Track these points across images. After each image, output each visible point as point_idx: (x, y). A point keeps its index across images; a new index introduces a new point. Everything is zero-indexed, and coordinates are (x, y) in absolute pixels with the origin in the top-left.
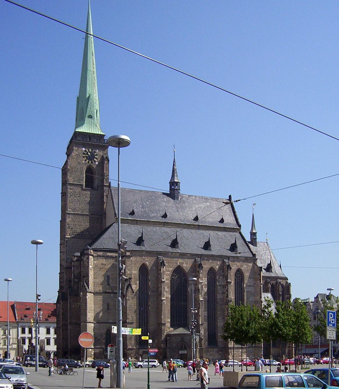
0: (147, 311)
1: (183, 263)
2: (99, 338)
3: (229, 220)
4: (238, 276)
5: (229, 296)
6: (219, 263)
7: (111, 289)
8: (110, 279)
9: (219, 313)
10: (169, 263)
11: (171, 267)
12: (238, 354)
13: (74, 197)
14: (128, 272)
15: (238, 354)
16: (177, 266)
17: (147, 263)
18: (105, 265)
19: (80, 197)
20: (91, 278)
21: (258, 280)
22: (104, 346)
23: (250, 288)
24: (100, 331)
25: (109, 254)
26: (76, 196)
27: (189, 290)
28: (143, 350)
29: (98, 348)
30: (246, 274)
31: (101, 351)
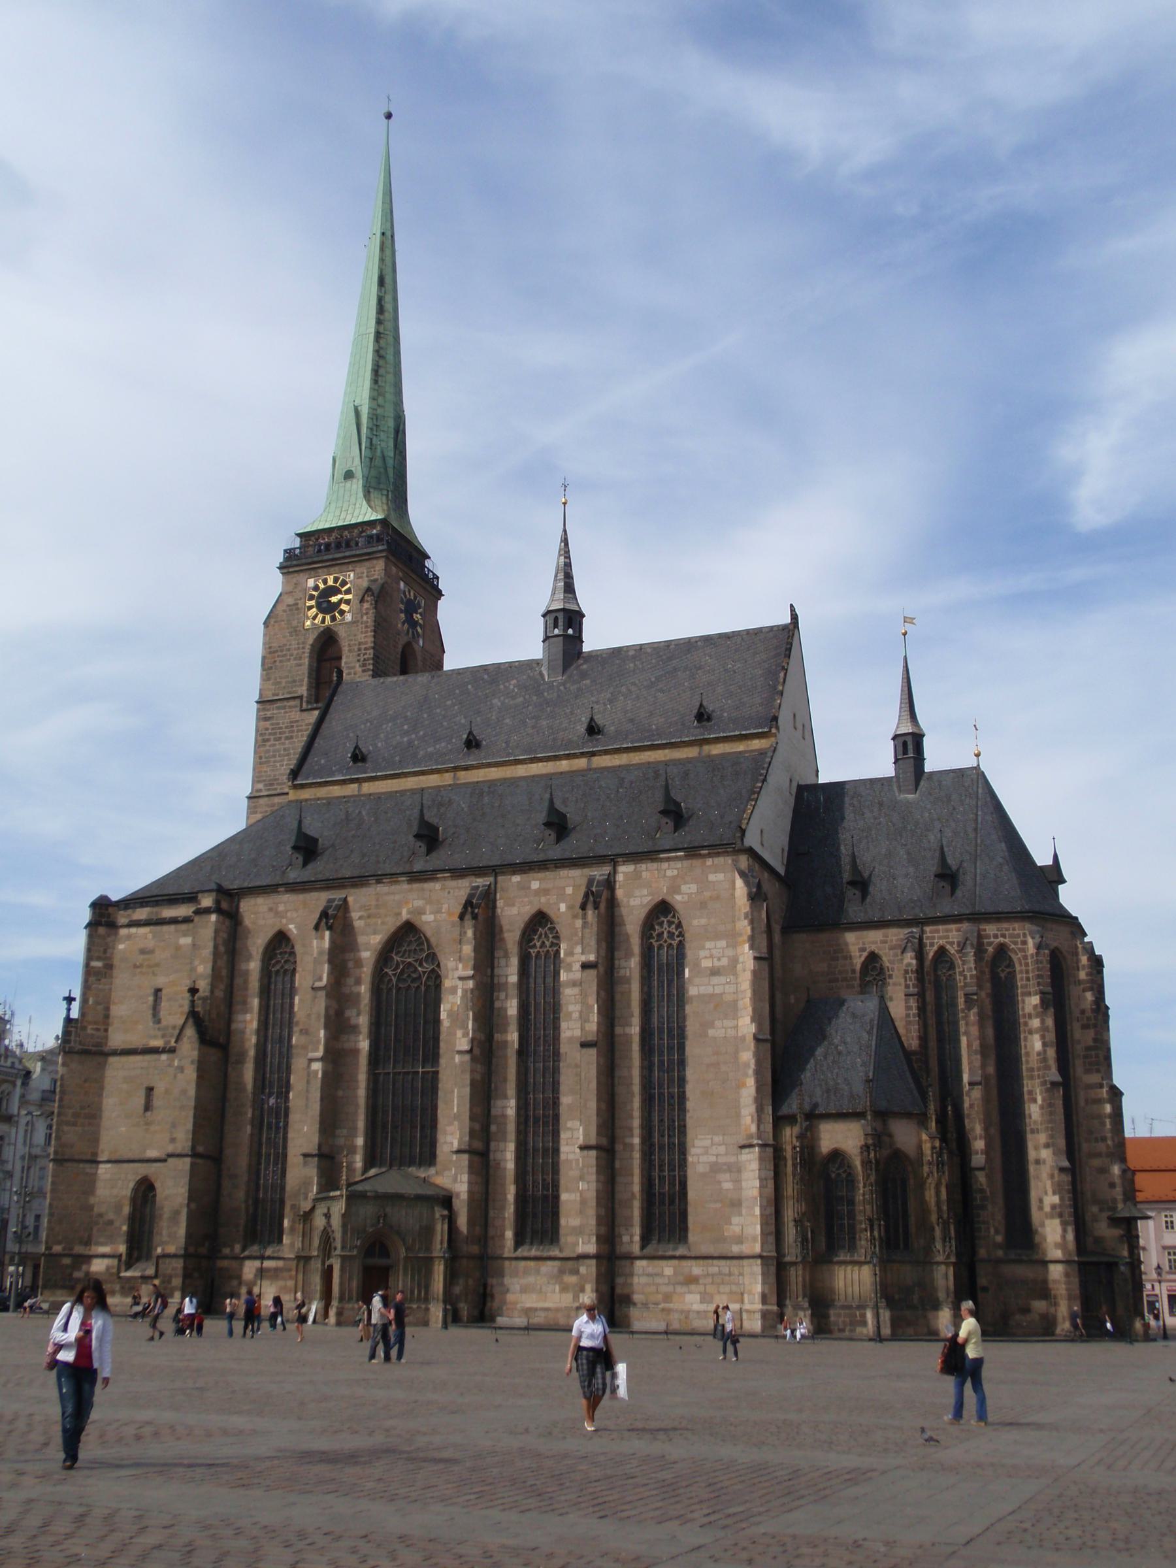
0: (287, 1109)
1: (421, 912)
2: (111, 1216)
4: (665, 935)
6: (569, 890)
7: (163, 1036)
8: (164, 998)
9: (566, 1100)
10: (369, 917)
11: (375, 934)
12: (653, 1289)
13: (272, 742)
14: (201, 969)
15: (653, 1289)
16: (399, 924)
17: (291, 926)
18: (152, 952)
19: (292, 737)
20: (97, 1003)
21: (744, 942)
22: (122, 1249)
23: (715, 980)
24: (115, 1192)
25: (168, 912)
26: (280, 738)
27: (443, 1015)
28: (257, 1263)
29: (104, 1256)
30: (695, 922)
31: (113, 1267)
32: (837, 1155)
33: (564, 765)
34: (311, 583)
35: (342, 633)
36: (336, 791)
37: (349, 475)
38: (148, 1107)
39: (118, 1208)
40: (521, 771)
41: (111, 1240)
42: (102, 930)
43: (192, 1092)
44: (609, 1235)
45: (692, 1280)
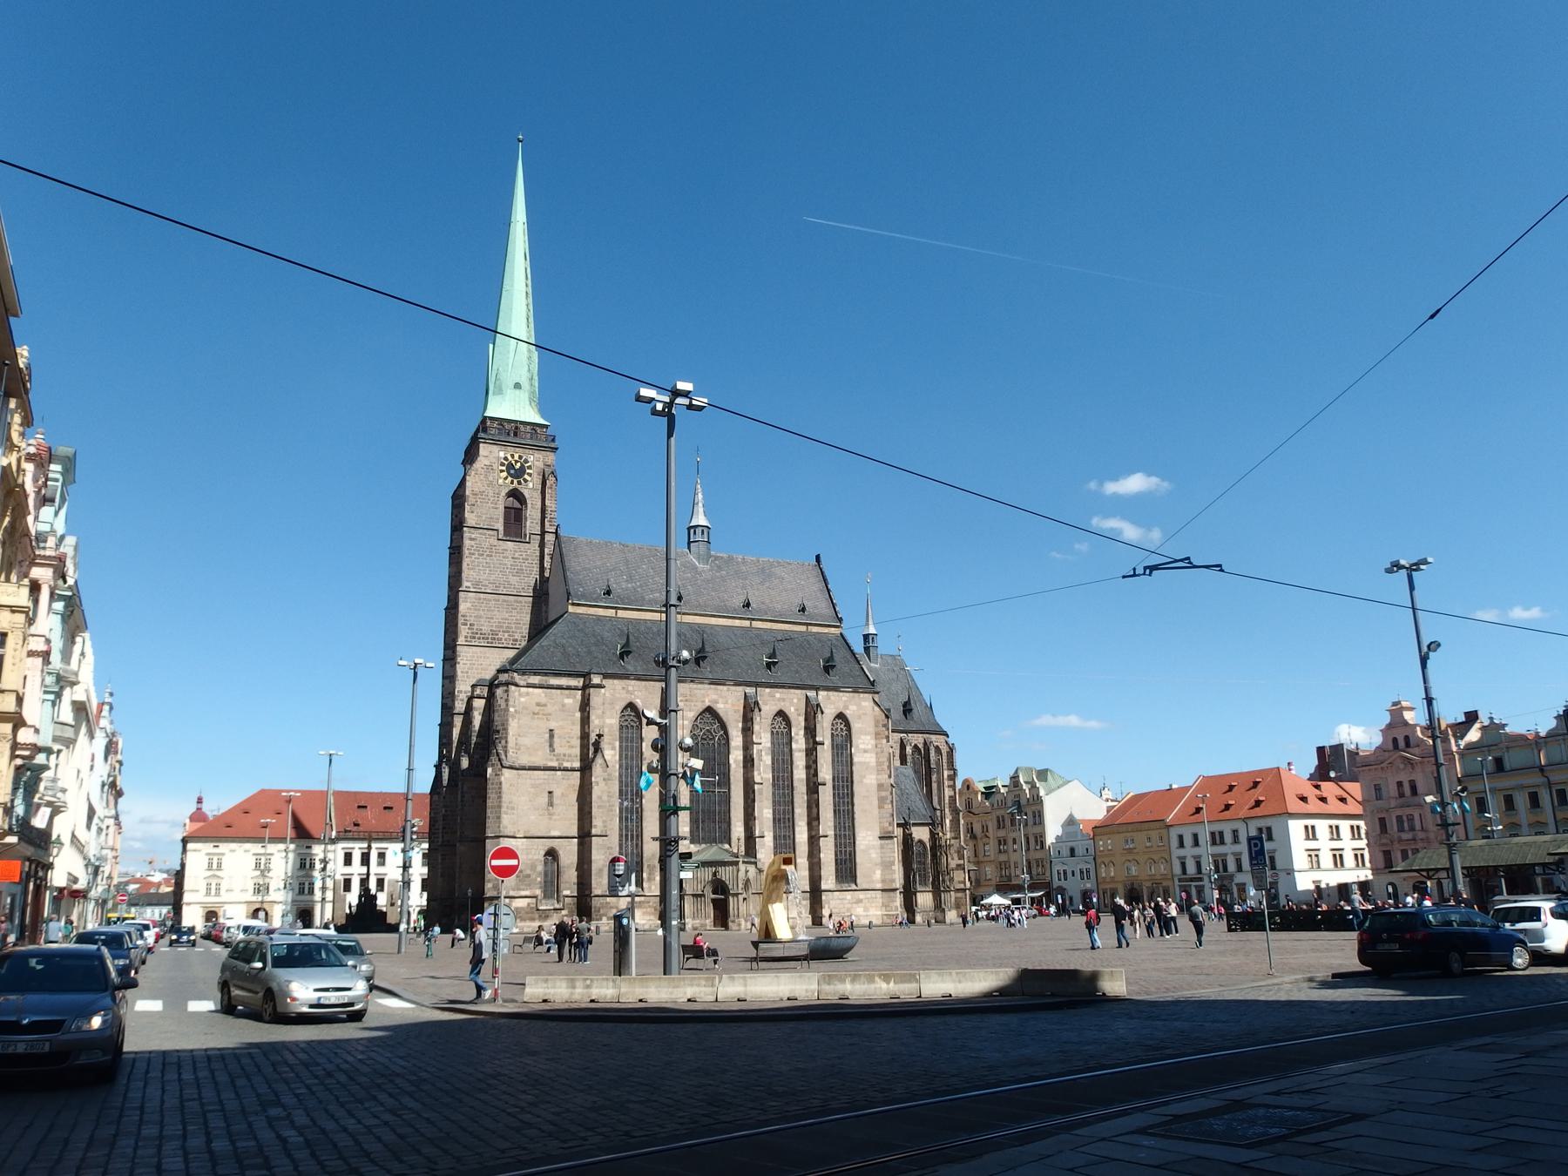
3: (818, 605)
5: (820, 775)
22: (538, 892)
25: (554, 681)
32: (920, 841)
33: (737, 623)
34: (502, 454)
35: (526, 493)
36: (601, 612)
37: (517, 386)
38: (551, 804)
39: (533, 867)
40: (713, 621)
41: (529, 886)
42: (513, 688)
43: (605, 798)
44: (815, 880)
45: (860, 901)
